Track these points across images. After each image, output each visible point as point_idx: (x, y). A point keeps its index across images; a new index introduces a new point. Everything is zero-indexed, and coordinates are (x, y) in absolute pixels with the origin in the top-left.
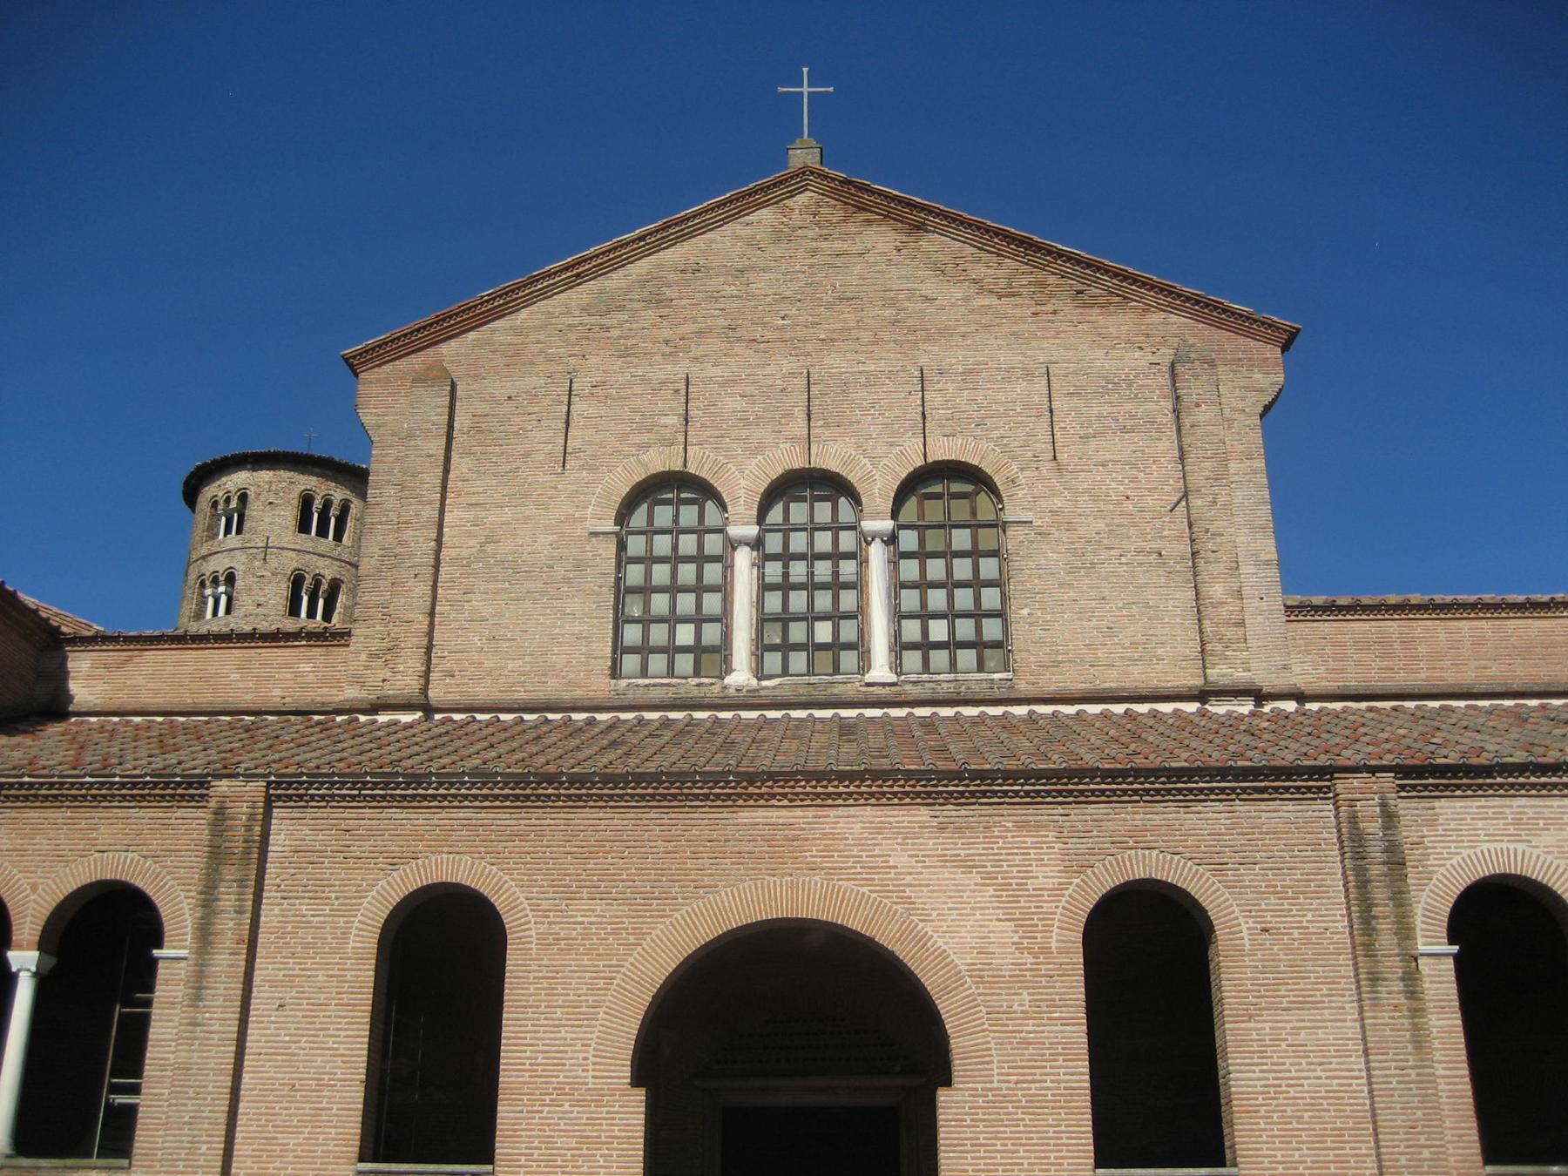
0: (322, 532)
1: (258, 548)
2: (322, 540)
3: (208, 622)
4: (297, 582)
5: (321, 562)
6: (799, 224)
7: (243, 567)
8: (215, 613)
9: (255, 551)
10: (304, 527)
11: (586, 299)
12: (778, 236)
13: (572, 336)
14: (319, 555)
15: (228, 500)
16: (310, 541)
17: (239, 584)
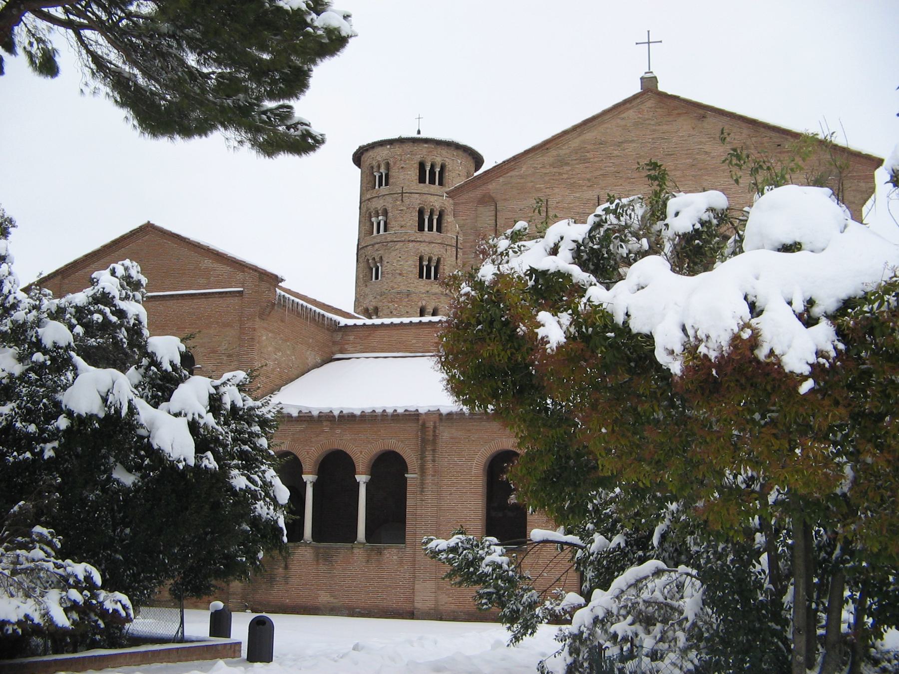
0: (432, 182)
2: (432, 186)
3: (374, 238)
4: (421, 212)
5: (432, 199)
6: (646, 117)
7: (391, 206)
8: (378, 231)
10: (422, 180)
11: (552, 159)
12: (636, 124)
13: (547, 179)
14: (431, 195)
15: (379, 167)
16: (426, 188)
17: (390, 214)
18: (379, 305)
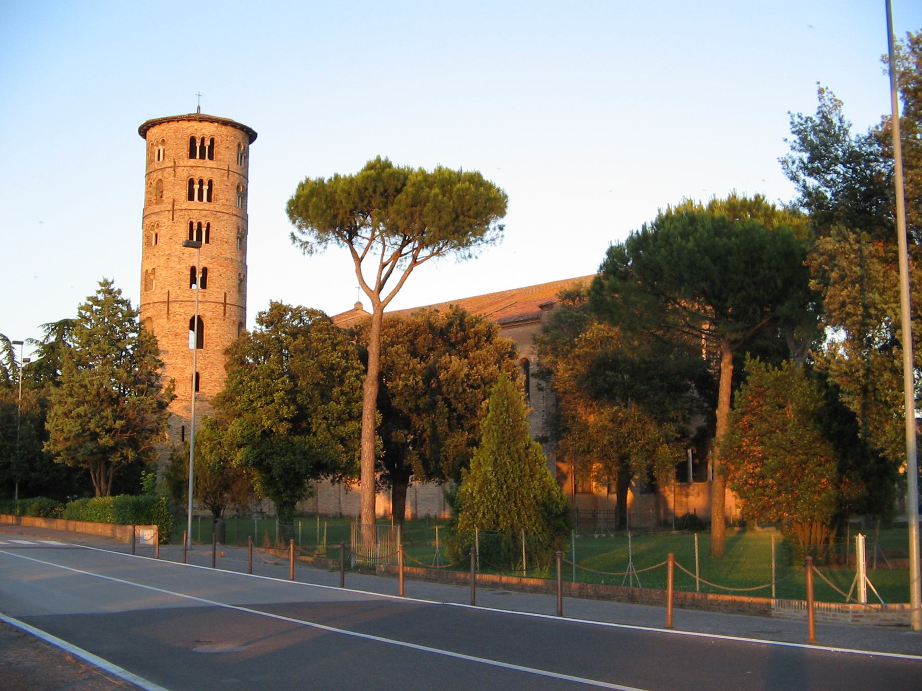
1: (225, 170)
8: (201, 199)
9: (224, 171)
18: (209, 266)
